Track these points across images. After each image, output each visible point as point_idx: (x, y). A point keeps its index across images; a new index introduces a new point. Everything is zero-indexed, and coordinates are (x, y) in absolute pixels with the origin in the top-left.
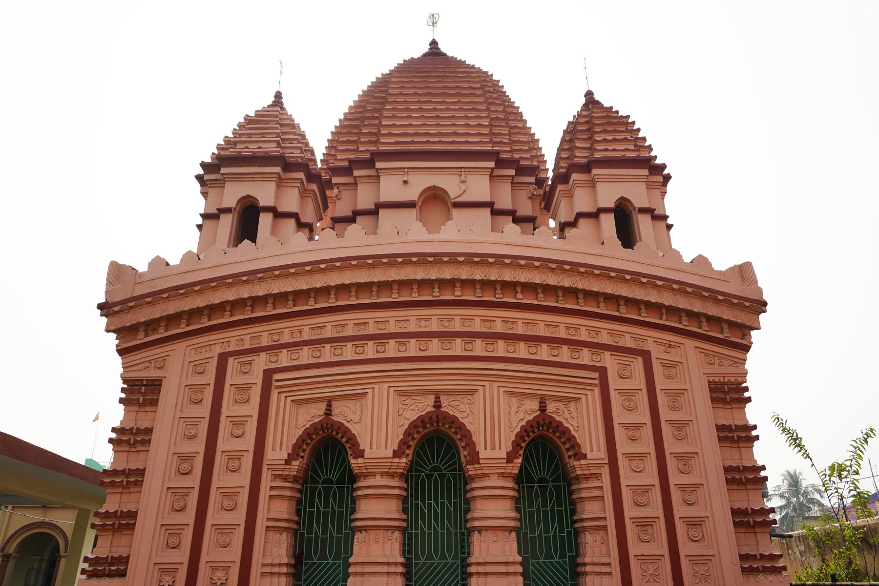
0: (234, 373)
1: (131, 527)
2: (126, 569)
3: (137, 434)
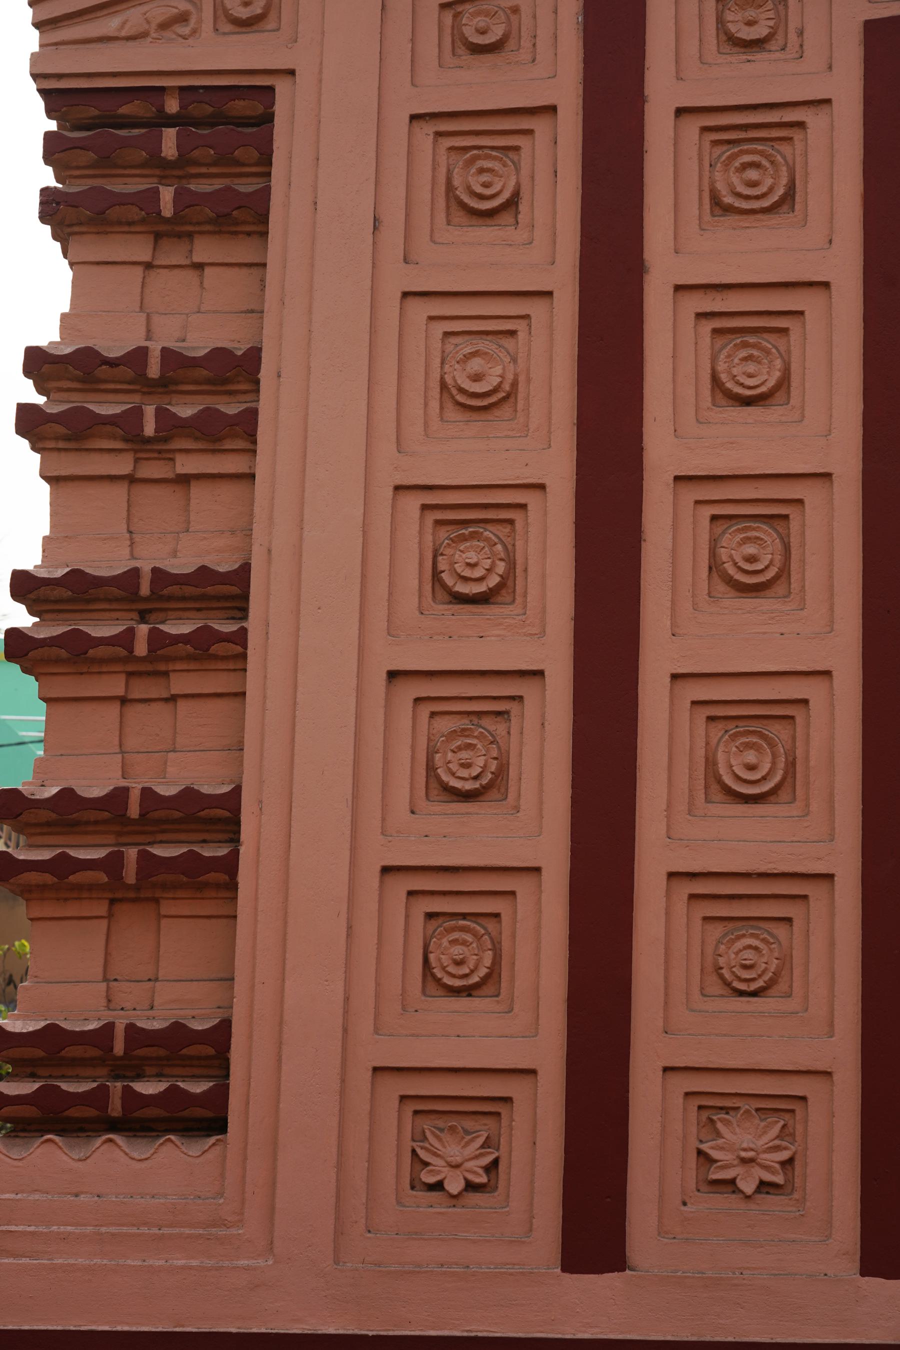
0: (691, 47)
1: (215, 880)
2: (219, 1097)
3: (164, 385)
